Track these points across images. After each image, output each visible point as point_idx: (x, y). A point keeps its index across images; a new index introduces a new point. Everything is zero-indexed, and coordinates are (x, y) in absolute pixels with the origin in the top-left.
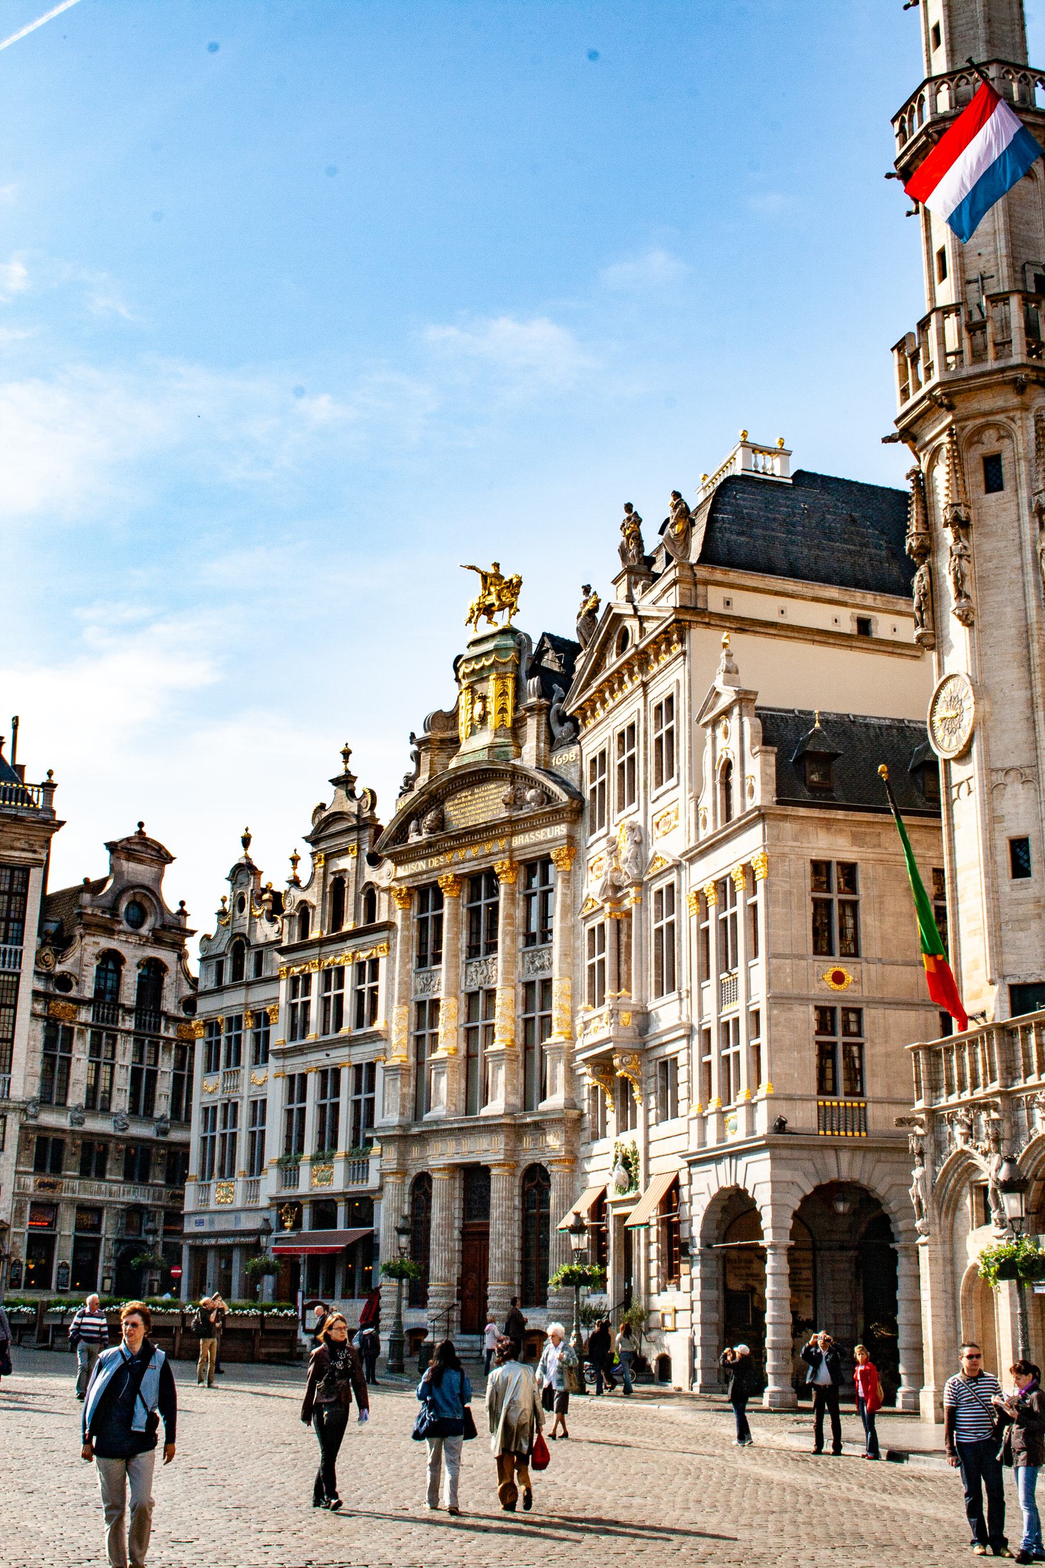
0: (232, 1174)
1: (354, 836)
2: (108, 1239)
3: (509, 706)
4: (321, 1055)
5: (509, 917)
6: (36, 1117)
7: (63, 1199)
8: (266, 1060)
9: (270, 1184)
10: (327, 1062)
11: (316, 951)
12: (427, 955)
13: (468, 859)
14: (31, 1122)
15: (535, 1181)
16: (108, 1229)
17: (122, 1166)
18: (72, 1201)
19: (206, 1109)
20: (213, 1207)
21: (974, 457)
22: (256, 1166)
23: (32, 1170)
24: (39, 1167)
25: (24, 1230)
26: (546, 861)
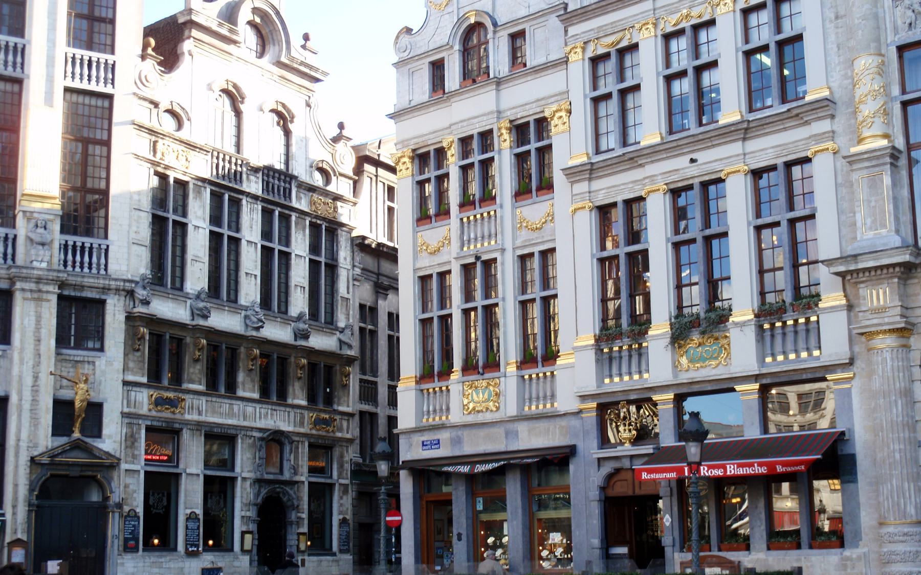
0: (492, 364)
2: (244, 479)
4: (682, 162)
6: (146, 303)
7: (187, 423)
8: (546, 186)
9: (577, 372)
10: (693, 171)
14: (141, 309)
16: (245, 464)
17: (257, 379)
18: (199, 425)
19: (424, 280)
20: (456, 417)
23: (144, 380)
24: (155, 376)
25: (140, 466)
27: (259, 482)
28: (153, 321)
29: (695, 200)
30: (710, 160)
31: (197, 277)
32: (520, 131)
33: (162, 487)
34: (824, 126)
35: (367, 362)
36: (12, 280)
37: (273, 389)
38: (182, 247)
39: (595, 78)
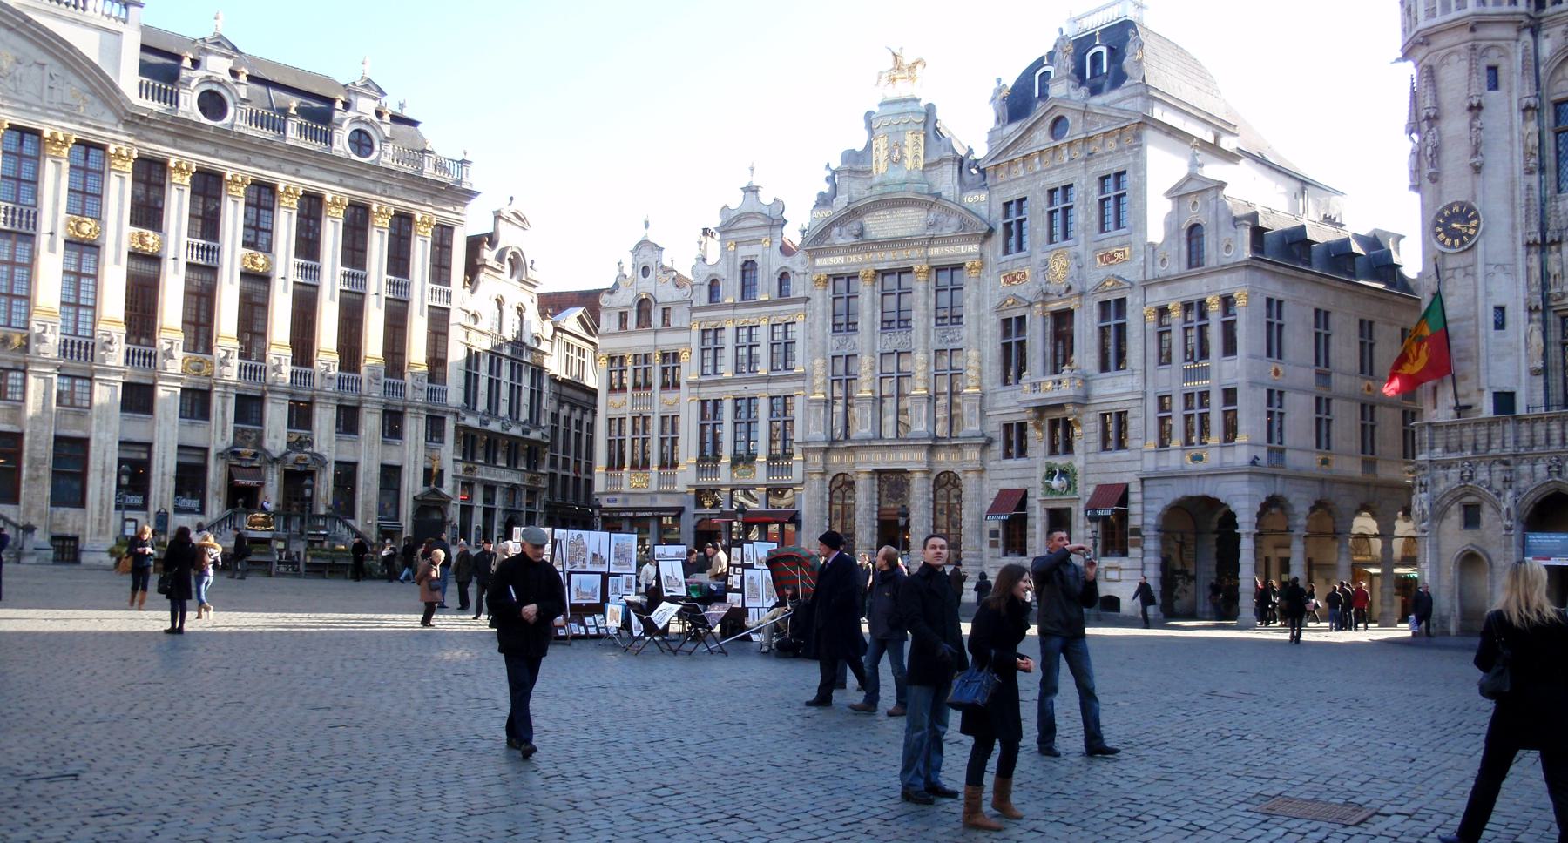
0: (646, 465)
1: (766, 231)
3: (921, 154)
4: (741, 387)
5: (926, 304)
11: (730, 312)
12: (845, 323)
13: (887, 259)
14: (461, 422)
15: (946, 483)
20: (625, 489)
21: (1484, 63)
22: (668, 463)
25: (458, 502)
26: (960, 267)
27: (505, 511)
28: (467, 428)
29: (744, 406)
30: (753, 389)
31: (482, 405)
32: (664, 356)
33: (466, 510)
34: (800, 384)
35: (554, 448)
36: (405, 407)
37: (512, 464)
38: (476, 387)
39: (703, 339)
